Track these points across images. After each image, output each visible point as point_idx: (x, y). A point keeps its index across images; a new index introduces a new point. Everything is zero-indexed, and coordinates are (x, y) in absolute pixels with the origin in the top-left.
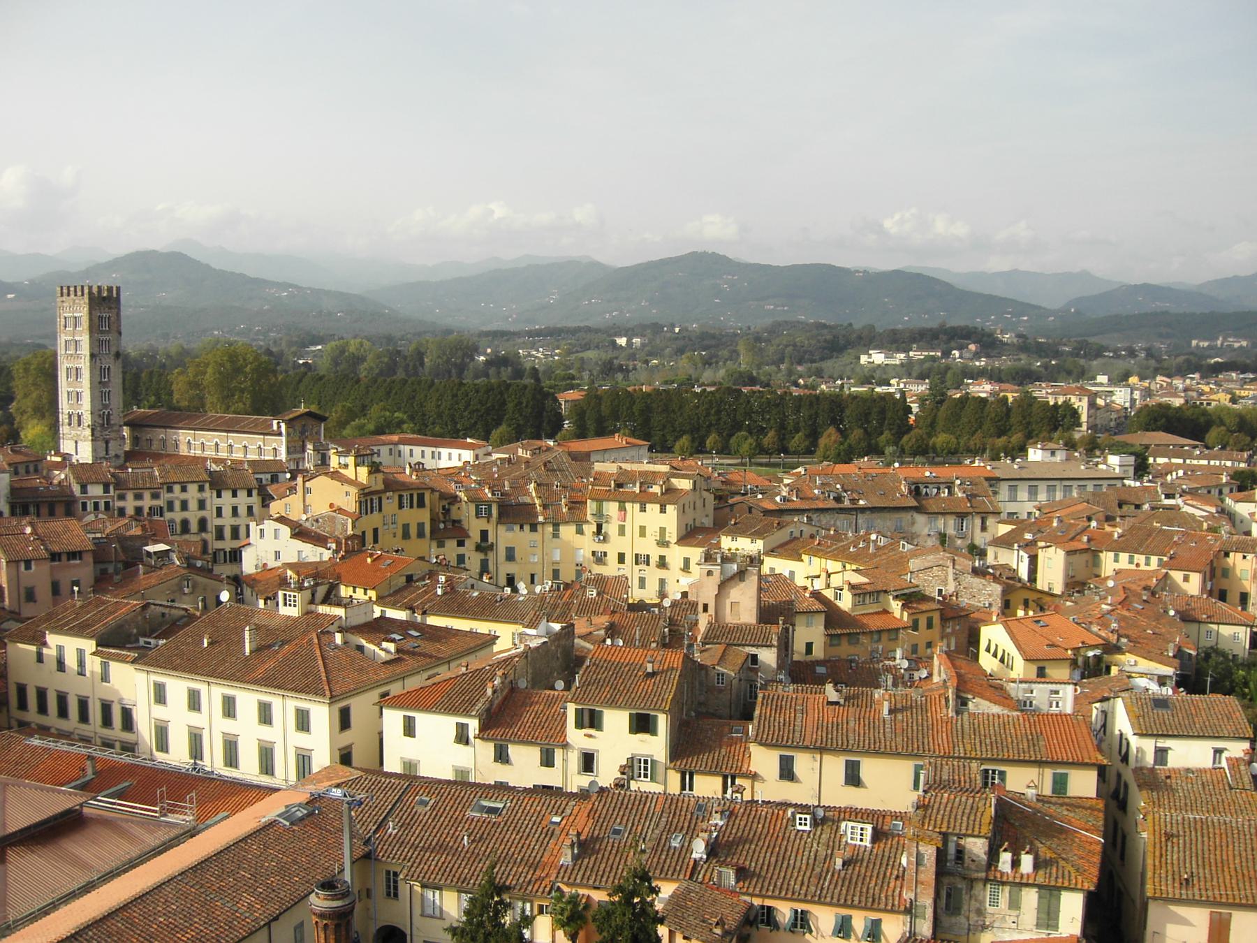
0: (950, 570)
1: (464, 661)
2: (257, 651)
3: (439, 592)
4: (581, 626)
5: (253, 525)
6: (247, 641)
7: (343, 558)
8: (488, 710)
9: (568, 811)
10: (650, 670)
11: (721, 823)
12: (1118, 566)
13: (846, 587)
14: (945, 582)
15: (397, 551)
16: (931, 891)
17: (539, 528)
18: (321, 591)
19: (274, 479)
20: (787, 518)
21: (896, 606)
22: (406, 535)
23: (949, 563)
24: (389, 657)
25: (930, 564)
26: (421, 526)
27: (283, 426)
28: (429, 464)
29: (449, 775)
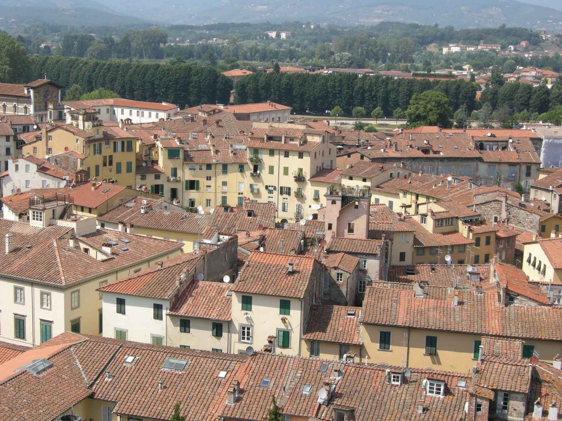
0: (504, 204)
1: (159, 260)
2: (15, 250)
3: (142, 211)
4: (242, 238)
5: (10, 162)
6: (7, 244)
7: (74, 186)
8: (176, 296)
9: (231, 368)
10: (290, 270)
11: (338, 379)
13: (429, 214)
14: (499, 212)
15: (113, 182)
17: (213, 167)
18: (59, 211)
19: (26, 129)
20: (387, 165)
21: (463, 229)
22: (119, 171)
23: (503, 199)
24: (105, 257)
25: (490, 199)
26: (129, 164)
27: (32, 92)
28: (135, 119)
29: (148, 340)
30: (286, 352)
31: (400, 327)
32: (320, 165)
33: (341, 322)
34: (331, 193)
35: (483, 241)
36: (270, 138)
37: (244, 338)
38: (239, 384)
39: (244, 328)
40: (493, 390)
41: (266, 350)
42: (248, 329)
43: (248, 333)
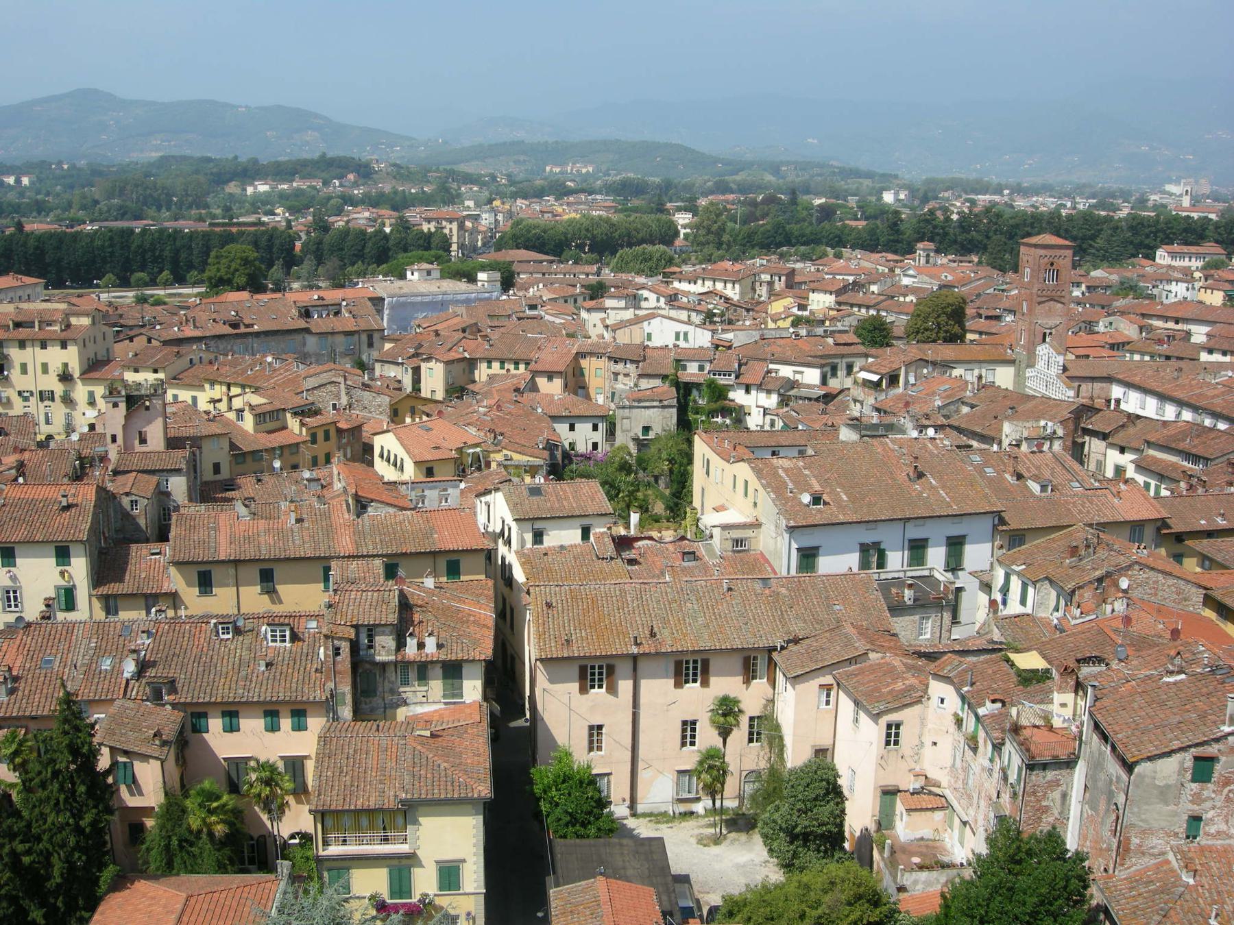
0: (342, 386)
10: (64, 503)
12: (490, 372)
13: (247, 408)
14: (338, 396)
16: (349, 679)
20: (184, 349)
21: (293, 423)
23: (341, 380)
25: (324, 381)
30: (71, 616)
31: (223, 562)
32: (92, 356)
33: (143, 566)
34: (111, 393)
35: (320, 436)
36: (18, 325)
37: (10, 606)
38: (10, 669)
39: (8, 592)
40: (352, 626)
41: (43, 618)
42: (15, 592)
43: (16, 598)
